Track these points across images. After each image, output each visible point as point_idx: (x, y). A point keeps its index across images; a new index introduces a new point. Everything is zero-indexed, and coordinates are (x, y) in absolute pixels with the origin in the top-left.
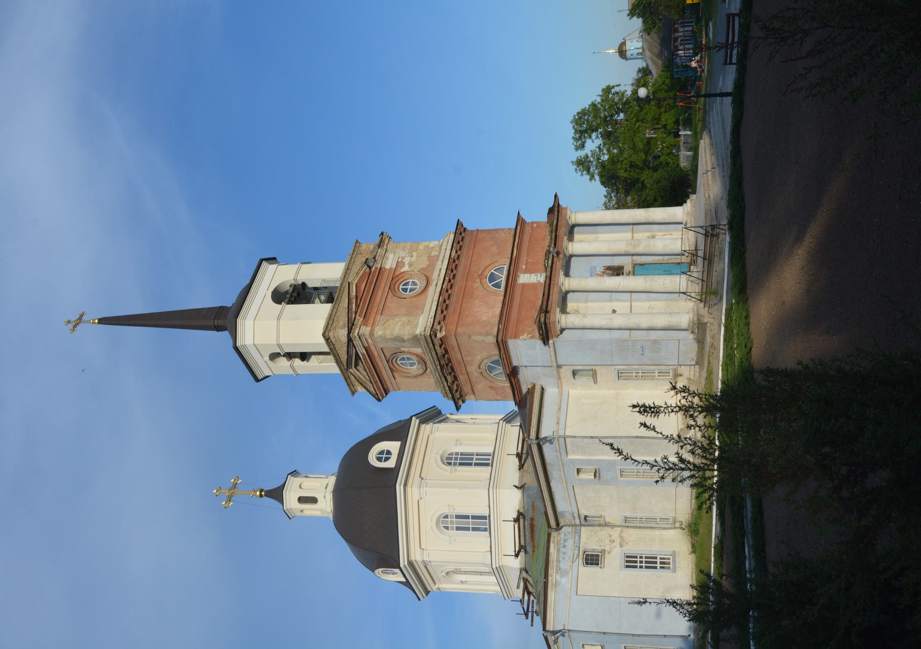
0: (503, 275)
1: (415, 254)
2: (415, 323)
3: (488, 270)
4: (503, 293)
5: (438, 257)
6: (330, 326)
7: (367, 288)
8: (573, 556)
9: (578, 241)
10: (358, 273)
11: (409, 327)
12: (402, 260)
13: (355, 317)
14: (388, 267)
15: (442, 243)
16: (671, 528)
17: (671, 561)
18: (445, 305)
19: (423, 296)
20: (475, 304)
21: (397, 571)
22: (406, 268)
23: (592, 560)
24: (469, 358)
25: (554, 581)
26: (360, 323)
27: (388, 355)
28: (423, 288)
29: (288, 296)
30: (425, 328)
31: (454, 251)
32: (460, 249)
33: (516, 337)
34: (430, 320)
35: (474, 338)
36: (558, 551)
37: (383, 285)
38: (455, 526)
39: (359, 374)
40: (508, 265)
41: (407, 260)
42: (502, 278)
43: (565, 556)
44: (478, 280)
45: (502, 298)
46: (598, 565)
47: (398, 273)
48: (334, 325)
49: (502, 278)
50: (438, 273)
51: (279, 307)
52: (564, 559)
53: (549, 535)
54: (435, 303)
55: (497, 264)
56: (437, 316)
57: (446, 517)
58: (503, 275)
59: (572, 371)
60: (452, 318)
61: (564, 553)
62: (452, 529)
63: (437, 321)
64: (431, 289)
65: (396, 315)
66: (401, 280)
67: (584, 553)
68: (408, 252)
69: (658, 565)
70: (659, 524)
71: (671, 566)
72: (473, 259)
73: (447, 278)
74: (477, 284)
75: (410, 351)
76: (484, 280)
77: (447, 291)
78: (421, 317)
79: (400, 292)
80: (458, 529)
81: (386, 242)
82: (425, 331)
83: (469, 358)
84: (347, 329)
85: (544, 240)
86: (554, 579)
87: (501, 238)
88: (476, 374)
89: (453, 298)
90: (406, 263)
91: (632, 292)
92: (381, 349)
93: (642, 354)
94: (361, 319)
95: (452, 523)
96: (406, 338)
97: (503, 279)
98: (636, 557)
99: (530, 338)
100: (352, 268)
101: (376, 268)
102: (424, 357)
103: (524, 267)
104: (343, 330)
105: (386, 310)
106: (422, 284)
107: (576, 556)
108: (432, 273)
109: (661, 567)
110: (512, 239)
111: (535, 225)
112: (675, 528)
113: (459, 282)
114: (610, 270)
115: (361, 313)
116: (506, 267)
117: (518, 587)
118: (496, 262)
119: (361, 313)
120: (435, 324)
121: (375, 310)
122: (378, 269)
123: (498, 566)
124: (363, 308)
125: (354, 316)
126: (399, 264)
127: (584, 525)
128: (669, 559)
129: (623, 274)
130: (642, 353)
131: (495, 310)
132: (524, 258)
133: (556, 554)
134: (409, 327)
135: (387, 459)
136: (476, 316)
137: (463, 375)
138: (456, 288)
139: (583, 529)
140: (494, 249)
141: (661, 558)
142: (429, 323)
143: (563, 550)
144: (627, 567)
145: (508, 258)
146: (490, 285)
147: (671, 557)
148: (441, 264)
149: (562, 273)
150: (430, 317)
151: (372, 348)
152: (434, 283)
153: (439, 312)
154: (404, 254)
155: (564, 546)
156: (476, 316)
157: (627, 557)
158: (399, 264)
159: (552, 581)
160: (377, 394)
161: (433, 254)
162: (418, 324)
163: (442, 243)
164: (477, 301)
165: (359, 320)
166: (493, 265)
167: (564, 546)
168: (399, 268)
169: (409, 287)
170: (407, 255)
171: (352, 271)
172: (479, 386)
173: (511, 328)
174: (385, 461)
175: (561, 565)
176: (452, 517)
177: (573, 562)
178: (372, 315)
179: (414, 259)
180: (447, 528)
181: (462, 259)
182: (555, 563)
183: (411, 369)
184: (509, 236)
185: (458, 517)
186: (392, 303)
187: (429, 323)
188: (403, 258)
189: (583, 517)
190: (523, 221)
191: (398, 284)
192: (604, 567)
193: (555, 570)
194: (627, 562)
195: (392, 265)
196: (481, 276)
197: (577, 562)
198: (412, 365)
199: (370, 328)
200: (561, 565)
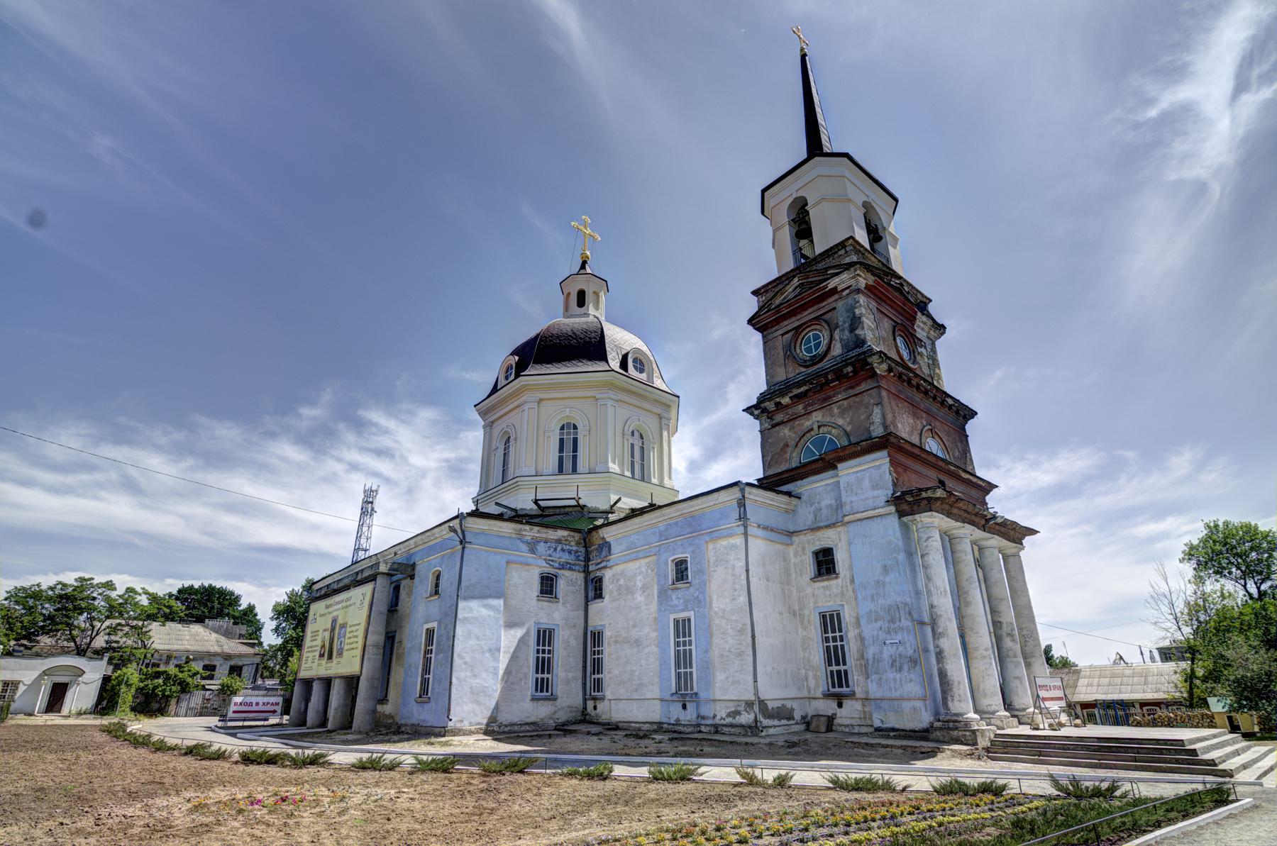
8: (552, 561)
16: (585, 694)
17: (545, 694)
21: (513, 377)
23: (548, 586)
24: (836, 411)
25: (524, 533)
27: (824, 317)
33: (893, 463)
35: (877, 410)
36: (559, 541)
38: (565, 437)
39: (790, 290)
43: (552, 550)
46: (541, 593)
53: (578, 531)
57: (575, 427)
59: (830, 546)
61: (555, 549)
62: (561, 434)
67: (556, 576)
69: (540, 676)
70: (591, 677)
71: (539, 694)
75: (834, 342)
80: (562, 441)
83: (836, 411)
86: (527, 533)
88: (810, 422)
92: (835, 308)
93: (885, 643)
95: (568, 434)
96: (858, 332)
98: (549, 645)
99: (893, 480)
102: (825, 360)
107: (552, 563)
109: (537, 679)
112: (585, 700)
115: (878, 284)
117: (497, 504)
118: (948, 453)
123: (519, 483)
127: (586, 578)
128: (547, 691)
130: (887, 642)
133: (556, 538)
135: (636, 368)
137: (805, 408)
139: (582, 575)
141: (548, 679)
143: (559, 548)
144: (539, 631)
147: (549, 693)
151: (836, 296)
155: (563, 550)
157: (550, 632)
159: (525, 530)
160: (760, 316)
167: (563, 550)
172: (786, 431)
173: (902, 458)
174: (634, 366)
175: (542, 544)
176: (577, 433)
177: (545, 560)
180: (562, 428)
182: (544, 536)
183: (801, 349)
185: (575, 441)
189: (598, 574)
190: (988, 492)
192: (538, 600)
194: (545, 632)
197: (545, 564)
198: (809, 350)
200: (542, 544)
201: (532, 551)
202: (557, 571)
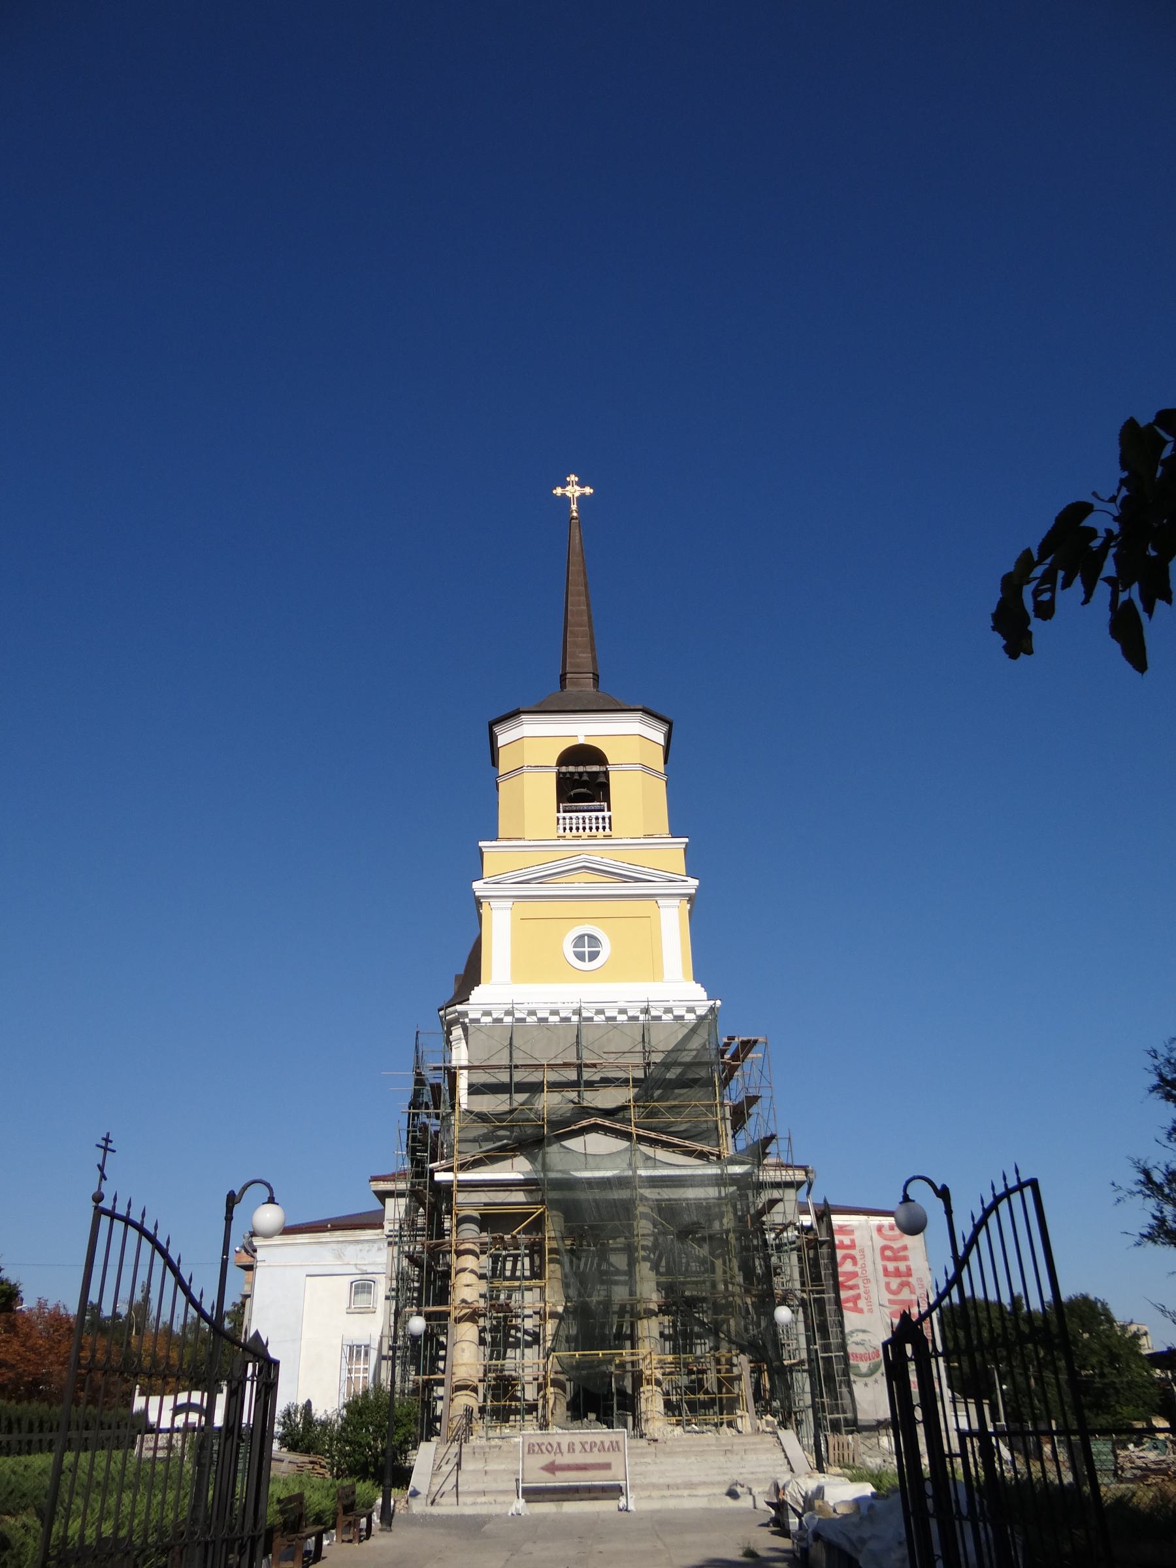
29: (581, 769)
51: (553, 762)
52: (361, 1250)
107: (364, 1268)
144: (351, 1347)
169: (586, 950)
193: (340, 1239)
201: (339, 1257)
202: (374, 1275)
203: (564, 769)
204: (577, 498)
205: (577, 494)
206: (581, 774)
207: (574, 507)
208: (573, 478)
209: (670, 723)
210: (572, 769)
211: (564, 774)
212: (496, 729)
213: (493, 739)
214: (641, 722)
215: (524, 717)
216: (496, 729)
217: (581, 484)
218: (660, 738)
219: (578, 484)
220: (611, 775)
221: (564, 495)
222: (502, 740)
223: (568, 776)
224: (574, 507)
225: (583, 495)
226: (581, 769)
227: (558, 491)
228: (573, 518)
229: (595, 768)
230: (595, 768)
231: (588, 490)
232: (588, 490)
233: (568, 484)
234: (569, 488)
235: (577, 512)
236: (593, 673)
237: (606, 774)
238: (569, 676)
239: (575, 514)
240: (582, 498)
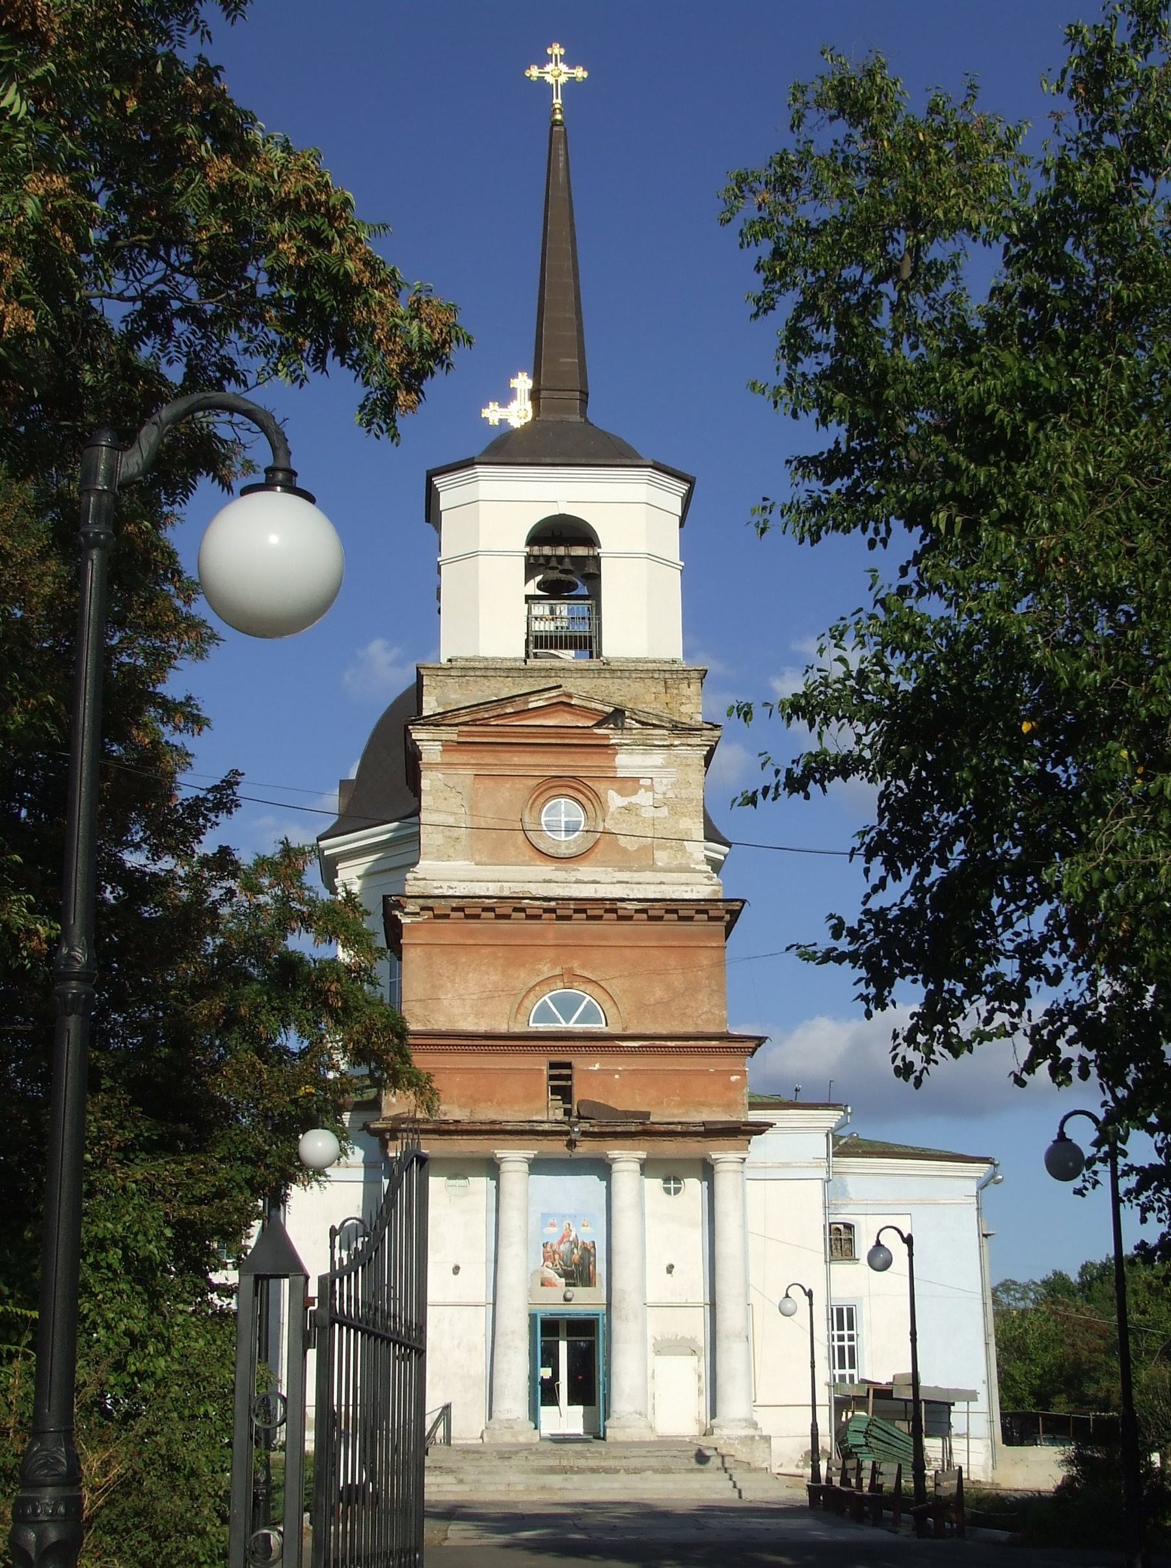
0: (576, 1022)
1: (664, 812)
2: (451, 851)
3: (590, 988)
4: (518, 1028)
5: (653, 868)
6: (447, 673)
7: (534, 730)
9: (641, 1181)
10: (591, 699)
11: (441, 841)
12: (642, 786)
13: (456, 725)
14: (621, 759)
15: (694, 871)
18: (478, 911)
19: (529, 853)
20: (487, 974)
22: (615, 800)
26: (444, 737)
28: (551, 851)
29: (561, 551)
30: (424, 879)
31: (640, 906)
32: (651, 918)
34: (445, 885)
37: (564, 760)
40: (606, 1030)
41: (643, 798)
42: (567, 1021)
44: (558, 971)
45: (502, 1028)
47: (598, 786)
48: (450, 681)
49: (567, 1021)
50: (586, 879)
51: (518, 543)
54: (492, 889)
55: (608, 1005)
56: (443, 902)
58: (576, 1022)
60: (449, 931)
63: (430, 903)
64: (547, 870)
65: (473, 807)
66: (580, 797)
68: (670, 794)
72: (628, 951)
73: (553, 904)
74: (546, 970)
76: (560, 984)
77: (516, 910)
78: (467, 862)
79: (547, 800)
81: (697, 741)
82: (416, 879)
84: (441, 710)
85: (682, 1104)
87: (693, 1004)
89: (504, 925)
90: (633, 799)
91: (713, 1305)
94: (455, 737)
97: (562, 1026)
100: (620, 678)
101: (606, 737)
103: (597, 1066)
104: (434, 704)
105: (490, 783)
106: (567, 848)
108: (604, 864)
110: (690, 1029)
111: (734, 1078)
113: (551, 930)
114: (582, 1258)
116: (599, 1027)
119: (471, 734)
120: (421, 901)
121: (489, 759)
122: (605, 742)
124: (485, 734)
125: (467, 719)
126: (630, 783)
129: (567, 1285)
131: (471, 1018)
132: (621, 1064)
134: (441, 841)
136: (453, 981)
138: (534, 925)
140: (659, 993)
142: (435, 884)
145: (624, 1029)
146: (546, 998)
148: (615, 880)
149: (531, 1154)
150: (453, 884)
152: (560, 875)
153: (454, 903)
154: (659, 788)
156: (453, 981)
158: (630, 784)
161: (662, 857)
162: (449, 858)
163: (694, 871)
164: (495, 977)
165: (451, 735)
166: (606, 997)
168: (617, 785)
170: (656, 796)
171: (611, 681)
178: (475, 755)
179: (649, 813)
181: (626, 926)
184: (699, 1021)
186: (508, 794)
187: (435, 884)
188: (650, 788)
191: (571, 792)
195: (623, 767)
196: (570, 977)
199: (439, 760)
203: (536, 550)
204: (564, 86)
205: (563, 79)
206: (560, 559)
207: (557, 102)
208: (557, 50)
209: (690, 481)
210: (547, 550)
211: (536, 557)
212: (438, 481)
213: (432, 496)
214: (650, 482)
215: (479, 469)
216: (438, 481)
217: (570, 60)
218: (677, 507)
219: (564, 59)
220: (604, 563)
221: (541, 80)
222: (446, 500)
223: (542, 561)
224: (557, 102)
225: (572, 80)
226: (561, 551)
227: (534, 72)
228: (555, 123)
229: (580, 551)
230: (580, 551)
231: (580, 73)
232: (580, 73)
233: (548, 59)
234: (550, 67)
235: (561, 112)
236: (581, 392)
237: (597, 559)
238: (544, 394)
239: (559, 117)
240: (571, 86)
